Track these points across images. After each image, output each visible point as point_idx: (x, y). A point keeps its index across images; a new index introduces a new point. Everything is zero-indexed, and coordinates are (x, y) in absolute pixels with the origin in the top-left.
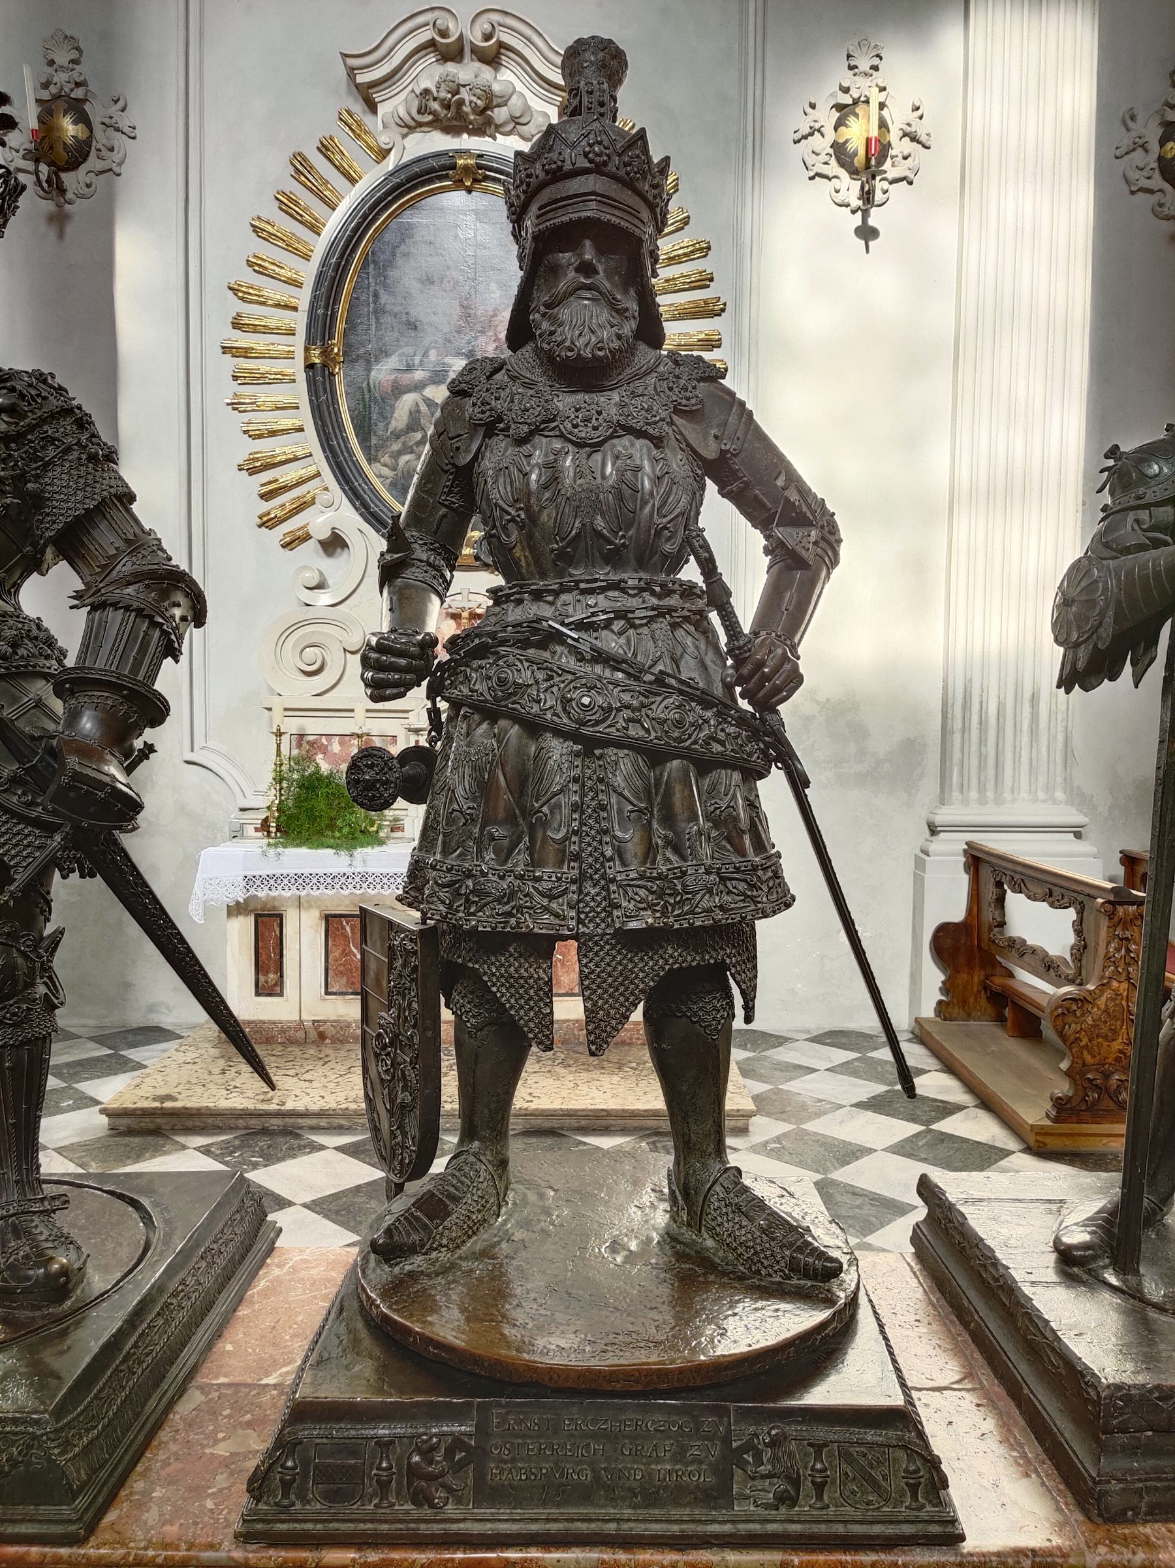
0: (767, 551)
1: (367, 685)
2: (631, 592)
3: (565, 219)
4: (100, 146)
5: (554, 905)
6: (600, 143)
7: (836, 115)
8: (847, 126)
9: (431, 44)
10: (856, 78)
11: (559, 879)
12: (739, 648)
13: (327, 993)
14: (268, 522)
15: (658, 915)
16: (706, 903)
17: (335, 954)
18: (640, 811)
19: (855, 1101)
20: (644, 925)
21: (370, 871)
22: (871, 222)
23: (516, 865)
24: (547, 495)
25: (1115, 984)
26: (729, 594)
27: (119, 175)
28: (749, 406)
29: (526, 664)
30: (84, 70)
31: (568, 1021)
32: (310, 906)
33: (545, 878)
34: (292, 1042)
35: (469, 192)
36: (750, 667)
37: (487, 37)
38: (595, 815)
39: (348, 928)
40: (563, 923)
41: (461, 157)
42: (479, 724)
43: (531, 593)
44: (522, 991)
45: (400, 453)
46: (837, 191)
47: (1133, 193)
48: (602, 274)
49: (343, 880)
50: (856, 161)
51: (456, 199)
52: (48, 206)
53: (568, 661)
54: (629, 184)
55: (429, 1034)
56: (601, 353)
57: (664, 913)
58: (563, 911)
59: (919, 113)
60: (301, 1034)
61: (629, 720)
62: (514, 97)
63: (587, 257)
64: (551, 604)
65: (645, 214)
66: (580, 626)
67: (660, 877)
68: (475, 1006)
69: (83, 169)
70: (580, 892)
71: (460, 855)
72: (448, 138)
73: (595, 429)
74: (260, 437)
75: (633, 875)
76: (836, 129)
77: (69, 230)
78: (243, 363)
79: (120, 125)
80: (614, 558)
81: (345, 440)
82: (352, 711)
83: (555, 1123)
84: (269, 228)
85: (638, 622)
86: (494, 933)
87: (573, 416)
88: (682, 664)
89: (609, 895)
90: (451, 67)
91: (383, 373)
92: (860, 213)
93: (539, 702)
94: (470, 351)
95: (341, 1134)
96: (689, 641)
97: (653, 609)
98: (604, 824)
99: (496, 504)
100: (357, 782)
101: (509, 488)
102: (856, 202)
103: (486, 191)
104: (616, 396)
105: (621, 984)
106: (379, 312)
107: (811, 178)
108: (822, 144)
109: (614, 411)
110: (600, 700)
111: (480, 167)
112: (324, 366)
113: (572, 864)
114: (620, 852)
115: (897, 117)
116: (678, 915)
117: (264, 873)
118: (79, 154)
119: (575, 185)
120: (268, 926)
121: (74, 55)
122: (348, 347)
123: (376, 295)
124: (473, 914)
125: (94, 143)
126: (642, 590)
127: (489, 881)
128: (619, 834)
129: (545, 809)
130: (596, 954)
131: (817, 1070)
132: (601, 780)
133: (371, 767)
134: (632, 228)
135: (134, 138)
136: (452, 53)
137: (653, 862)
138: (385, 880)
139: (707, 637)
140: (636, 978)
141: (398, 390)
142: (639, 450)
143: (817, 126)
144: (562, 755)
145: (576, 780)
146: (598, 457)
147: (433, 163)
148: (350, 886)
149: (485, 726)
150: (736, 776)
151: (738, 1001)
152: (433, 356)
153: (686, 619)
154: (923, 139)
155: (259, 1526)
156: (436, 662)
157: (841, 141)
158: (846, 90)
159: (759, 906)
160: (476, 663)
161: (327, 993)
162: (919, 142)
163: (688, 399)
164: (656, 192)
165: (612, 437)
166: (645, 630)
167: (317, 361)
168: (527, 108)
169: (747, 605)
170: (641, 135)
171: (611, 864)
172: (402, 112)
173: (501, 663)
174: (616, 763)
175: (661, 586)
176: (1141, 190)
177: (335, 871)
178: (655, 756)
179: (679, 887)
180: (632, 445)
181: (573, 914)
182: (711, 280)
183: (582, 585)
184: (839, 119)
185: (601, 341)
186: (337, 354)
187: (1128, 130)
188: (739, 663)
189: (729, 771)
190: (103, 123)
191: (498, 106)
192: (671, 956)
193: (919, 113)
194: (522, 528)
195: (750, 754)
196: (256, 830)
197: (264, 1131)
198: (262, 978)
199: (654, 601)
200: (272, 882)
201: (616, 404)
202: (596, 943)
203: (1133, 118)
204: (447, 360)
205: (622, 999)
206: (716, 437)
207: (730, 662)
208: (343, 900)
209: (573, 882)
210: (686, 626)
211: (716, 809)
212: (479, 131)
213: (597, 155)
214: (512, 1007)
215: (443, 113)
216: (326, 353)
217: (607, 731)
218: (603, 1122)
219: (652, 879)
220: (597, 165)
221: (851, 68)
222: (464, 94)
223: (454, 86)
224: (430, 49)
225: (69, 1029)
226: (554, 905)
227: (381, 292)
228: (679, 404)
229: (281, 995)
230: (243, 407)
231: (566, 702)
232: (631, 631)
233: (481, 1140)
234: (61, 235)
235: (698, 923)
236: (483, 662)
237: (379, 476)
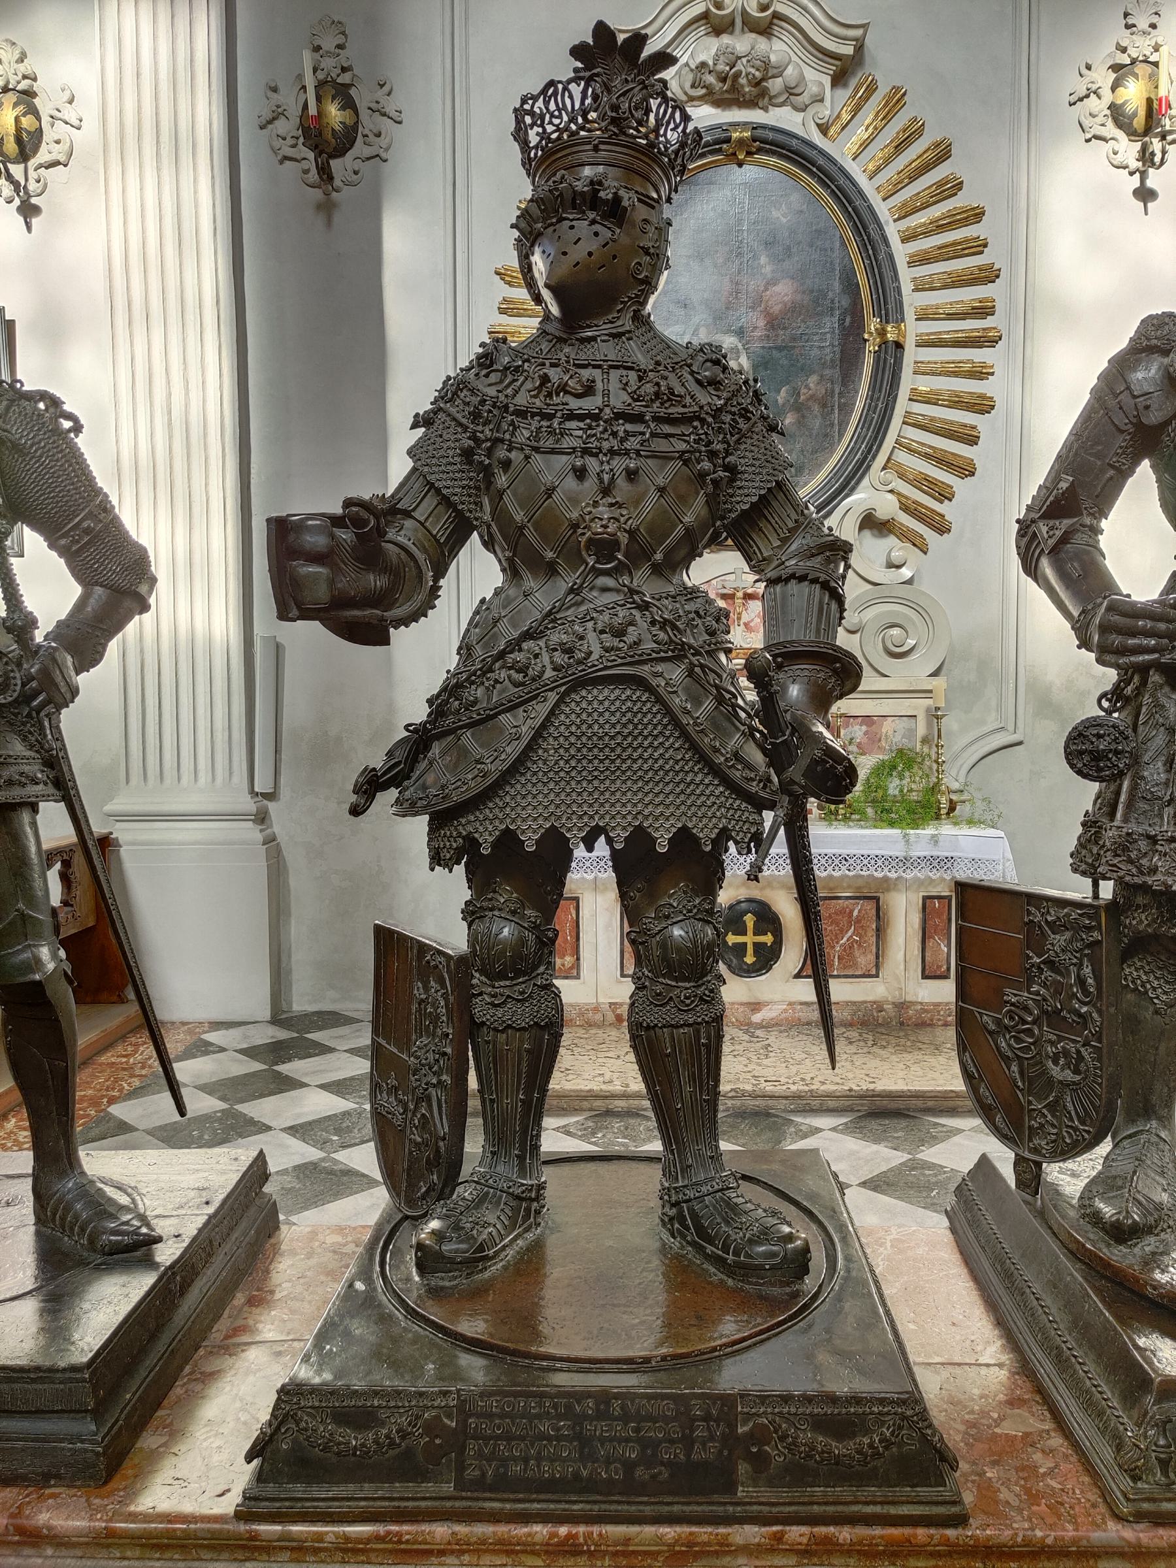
4: (366, 132)
7: (1112, 76)
9: (705, 16)
27: (385, 161)
30: (350, 55)
31: (866, 1002)
34: (590, 1025)
35: (740, 165)
41: (736, 131)
46: (1115, 153)
50: (1135, 122)
52: (317, 194)
60: (598, 1017)
62: (790, 68)
72: (719, 111)
76: (1113, 89)
77: (337, 218)
79: (387, 110)
83: (900, 1104)
90: (726, 39)
92: (1138, 174)
94: (742, 327)
102: (1135, 165)
107: (1088, 141)
118: (345, 141)
121: (340, 40)
135: (400, 123)
143: (1094, 87)
155: (1146, 1506)
157: (1119, 102)
158: (1124, 50)
161: (623, 975)
168: (802, 78)
182: (985, 246)
190: (369, 108)
191: (774, 77)
197: (609, 1113)
212: (751, 104)
215: (718, 86)
218: (951, 1104)
221: (1128, 27)
223: (733, 58)
229: (578, 977)
234: (329, 223)
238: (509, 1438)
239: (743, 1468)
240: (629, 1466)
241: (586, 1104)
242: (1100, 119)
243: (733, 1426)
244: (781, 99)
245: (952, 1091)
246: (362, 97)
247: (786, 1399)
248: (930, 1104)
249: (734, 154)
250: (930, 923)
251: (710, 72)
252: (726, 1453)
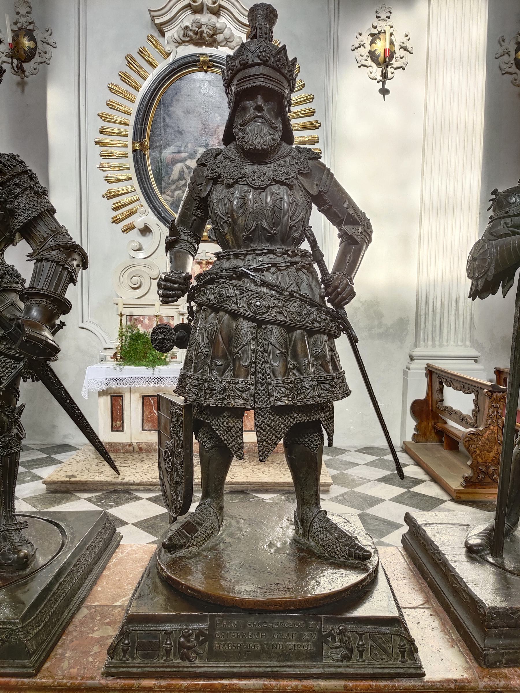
0: (340, 236)
1: (160, 296)
2: (278, 255)
3: (249, 86)
4: (40, 51)
5: (244, 395)
6: (265, 51)
7: (370, 38)
8: (376, 44)
9: (189, 6)
10: (380, 22)
11: (246, 383)
12: (327, 280)
13: (143, 430)
14: (116, 221)
15: (290, 399)
16: (312, 394)
17: (147, 413)
18: (282, 353)
19: (377, 478)
20: (284, 404)
21: (162, 376)
22: (386, 87)
23: (227, 377)
24: (241, 211)
25: (492, 427)
26: (322, 256)
27: (49, 64)
28: (331, 171)
29: (232, 287)
30: (33, 17)
31: (249, 443)
32: (135, 392)
33: (240, 383)
34: (127, 452)
36: (332, 288)
38: (262, 355)
39: (152, 402)
40: (248, 403)
41: (202, 57)
42: (210, 314)
43: (234, 255)
44: (229, 433)
45: (175, 190)
46: (371, 73)
47: (503, 74)
48: (266, 111)
49: (150, 380)
50: (379, 59)
51: (200, 75)
52: (17, 78)
53: (250, 286)
54: (278, 70)
55: (188, 451)
56: (265, 147)
57: (293, 399)
58: (248, 397)
59: (408, 38)
60: (131, 448)
61: (278, 312)
62: (226, 30)
63: (259, 103)
64: (243, 260)
65: (285, 84)
66: (255, 270)
67: (291, 382)
68: (209, 439)
69: (33, 61)
70: (256, 389)
71: (202, 372)
72: (196, 48)
73: (263, 181)
74: (112, 182)
75: (279, 382)
76: (370, 45)
77: (27, 89)
78: (105, 149)
79: (49, 42)
80: (271, 239)
81: (151, 184)
82: (154, 305)
84: (116, 88)
85: (281, 268)
86: (217, 407)
87: (253, 176)
88: (301, 288)
89: (268, 390)
90: (198, 16)
91: (167, 154)
92: (381, 83)
93: (237, 304)
94: (207, 144)
95: (149, 493)
96: (304, 277)
97: (289, 262)
98: (266, 359)
99: (218, 215)
100: (156, 339)
101: (224, 208)
102: (379, 78)
103: (213, 72)
104: (272, 166)
105: (274, 430)
106: (166, 126)
107: (360, 67)
108: (365, 51)
109: (271, 173)
110: (265, 304)
111: (210, 61)
112: (141, 151)
113: (252, 377)
114: (273, 371)
115: (398, 40)
116: (299, 399)
117: (115, 377)
118: (31, 55)
119: (253, 71)
120: (116, 401)
121: (28, 10)
122: (152, 142)
123: (164, 119)
124: (208, 399)
125: (37, 49)
126: (283, 254)
127: (215, 384)
128: (273, 363)
129: (240, 352)
130: (263, 417)
131: (360, 465)
132: (265, 339)
133: (162, 333)
134: (279, 90)
135: (55, 48)
136: (198, 10)
137: (288, 376)
138: (169, 380)
139: (313, 275)
140: (280, 427)
141: (174, 162)
142: (282, 191)
143: (362, 43)
144: (247, 328)
145: (254, 339)
146: (264, 194)
147: (190, 59)
148: (153, 383)
149: (213, 314)
150: (325, 337)
151: (326, 437)
152: (190, 146)
153: (303, 267)
154: (410, 49)
156: (191, 286)
157: (373, 50)
158: (375, 27)
159: (335, 395)
160: (209, 286)
161: (143, 430)
162: (408, 51)
163: (304, 168)
164: (290, 73)
165: (270, 185)
166: (285, 272)
167: (138, 148)
168: (232, 35)
169: (330, 260)
170: (284, 48)
171: (269, 376)
172: (176, 36)
173: (220, 286)
174: (272, 331)
175: (292, 252)
176: (507, 73)
177: (146, 376)
178: (289, 328)
179: (300, 387)
180: (279, 189)
181: (252, 399)
182: (314, 112)
183: (257, 252)
184: (372, 40)
185: (266, 142)
186: (147, 145)
187: (501, 46)
188: (327, 287)
189: (322, 335)
190: (42, 41)
191: (219, 34)
192: (296, 417)
193: (408, 38)
194: (230, 226)
195: (331, 328)
196: (111, 358)
197: (115, 491)
198: (114, 424)
199: (289, 259)
200: (118, 381)
201: (272, 170)
202: (263, 412)
203: (503, 40)
204: (197, 148)
205: (274, 436)
206: (317, 185)
207: (323, 286)
208: (150, 389)
209: (252, 384)
210: (303, 270)
211: (316, 352)
212: (210, 45)
213: (264, 57)
214: (225, 440)
215: (194, 37)
216: (142, 145)
217: (267, 317)
218: (265, 488)
219: (287, 383)
220: (264, 61)
221: (377, 17)
222: (204, 28)
223: (199, 25)
224: (189, 8)
225: (29, 446)
226: (244, 395)
227: (167, 117)
228: (300, 170)
229: (123, 431)
230: (105, 169)
231: (249, 304)
232: (279, 272)
233: (211, 498)
234: (23, 91)
235: (308, 403)
236: (212, 286)
237: (166, 200)
241: (105, 488)
242: (365, 58)
245: (265, 482)
246: (38, 35)
248: (257, 488)
249: (202, 67)
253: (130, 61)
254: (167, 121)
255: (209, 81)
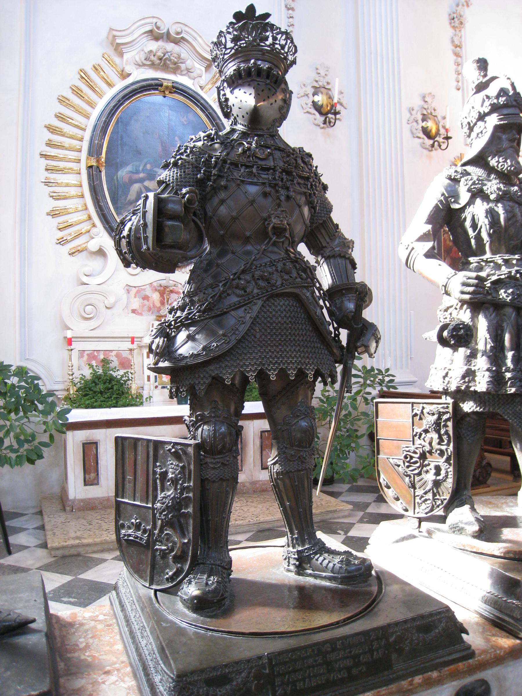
9: (151, 31)
14: (61, 242)
37: (178, 33)
74: (58, 199)
76: (313, 95)
91: (123, 173)
111: (173, 87)
112: (98, 167)
123: (122, 138)
141: (132, 182)
152: (148, 167)
154: (345, 105)
172: (138, 59)
187: (411, 114)
191: (181, 63)
198: (87, 476)
204: (156, 169)
222: (167, 56)
229: (98, 484)
230: (51, 184)
238: (295, 671)
239: (394, 656)
240: (349, 669)
243: (387, 639)
244: (185, 72)
247: (405, 622)
249: (164, 92)
250: (264, 443)
251: (154, 55)
252: (386, 652)
253: (84, 76)
254: (124, 140)
255: (169, 106)
